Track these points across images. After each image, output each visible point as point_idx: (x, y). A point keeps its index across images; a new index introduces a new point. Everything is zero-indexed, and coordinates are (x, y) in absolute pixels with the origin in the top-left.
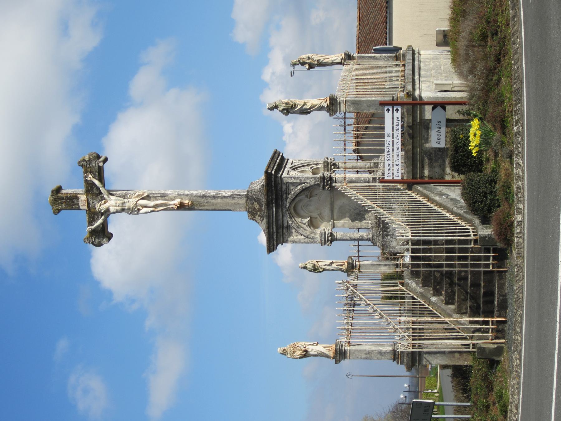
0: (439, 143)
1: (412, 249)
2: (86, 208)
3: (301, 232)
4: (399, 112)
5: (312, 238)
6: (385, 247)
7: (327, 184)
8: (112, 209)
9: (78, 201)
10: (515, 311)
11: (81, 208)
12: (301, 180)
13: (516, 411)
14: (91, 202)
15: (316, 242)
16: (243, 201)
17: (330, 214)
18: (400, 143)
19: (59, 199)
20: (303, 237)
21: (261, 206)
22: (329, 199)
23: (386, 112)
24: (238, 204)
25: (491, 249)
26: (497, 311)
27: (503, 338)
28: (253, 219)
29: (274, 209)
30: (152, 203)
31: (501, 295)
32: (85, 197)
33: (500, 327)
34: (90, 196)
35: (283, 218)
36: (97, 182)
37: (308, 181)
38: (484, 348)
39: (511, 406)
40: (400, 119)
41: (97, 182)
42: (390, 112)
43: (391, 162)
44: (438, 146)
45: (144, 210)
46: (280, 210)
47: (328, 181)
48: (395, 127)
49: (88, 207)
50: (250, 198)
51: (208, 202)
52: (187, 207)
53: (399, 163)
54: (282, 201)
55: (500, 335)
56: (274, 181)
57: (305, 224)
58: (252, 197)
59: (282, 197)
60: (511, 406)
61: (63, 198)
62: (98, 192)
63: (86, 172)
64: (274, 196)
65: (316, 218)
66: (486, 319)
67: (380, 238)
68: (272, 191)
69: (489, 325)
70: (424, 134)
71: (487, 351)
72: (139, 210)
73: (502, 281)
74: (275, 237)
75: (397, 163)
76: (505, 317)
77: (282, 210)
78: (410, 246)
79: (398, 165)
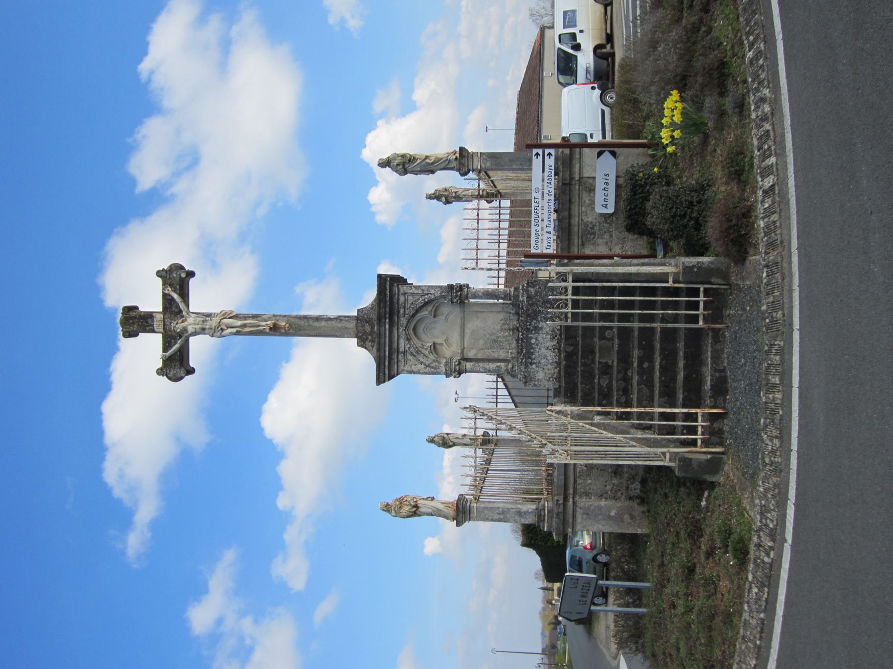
0: (605, 206)
1: (573, 288)
2: (162, 330)
3: (422, 360)
4: (553, 158)
5: (435, 368)
6: (529, 379)
7: (456, 296)
8: (191, 329)
9: (153, 321)
10: (766, 348)
11: (156, 330)
12: (423, 290)
13: (770, 544)
14: (167, 323)
15: (439, 373)
16: (352, 325)
17: (459, 340)
18: (553, 202)
19: (131, 318)
20: (423, 366)
21: (372, 328)
22: (459, 320)
23: (534, 158)
24: (346, 328)
25: (702, 289)
26: (710, 397)
27: (721, 444)
28: (362, 346)
29: (387, 326)
30: (239, 323)
31: (716, 370)
32: (162, 316)
33: (715, 425)
34: (168, 315)
35: (398, 340)
36: (175, 296)
37: (433, 292)
38: (690, 459)
39: (759, 537)
40: (553, 168)
41: (175, 296)
42: (540, 158)
43: (539, 228)
44: (605, 211)
45: (230, 330)
46: (395, 328)
47: (457, 292)
48: (546, 178)
49: (164, 329)
50: (362, 318)
51: (309, 325)
52: (283, 331)
53: (551, 229)
54: (398, 317)
55: (715, 439)
56: (388, 288)
57: (426, 349)
58: (363, 317)
59: (399, 312)
60: (759, 537)
61: (135, 317)
62: (177, 310)
63: (164, 284)
64: (388, 309)
65: (441, 344)
66: (693, 411)
67: (523, 368)
68: (386, 302)
69: (697, 421)
70: (584, 198)
71: (695, 465)
72: (222, 330)
73: (718, 346)
74: (387, 363)
75: (548, 229)
76: (724, 408)
77: (398, 329)
78: (570, 284)
79: (549, 233)
